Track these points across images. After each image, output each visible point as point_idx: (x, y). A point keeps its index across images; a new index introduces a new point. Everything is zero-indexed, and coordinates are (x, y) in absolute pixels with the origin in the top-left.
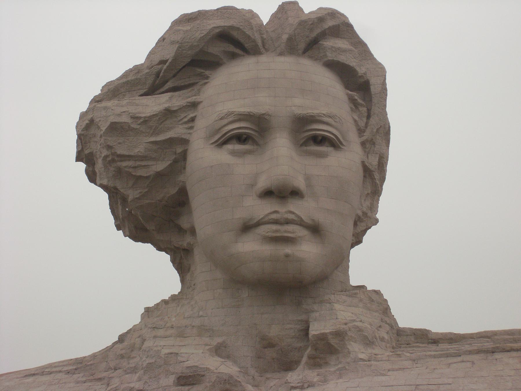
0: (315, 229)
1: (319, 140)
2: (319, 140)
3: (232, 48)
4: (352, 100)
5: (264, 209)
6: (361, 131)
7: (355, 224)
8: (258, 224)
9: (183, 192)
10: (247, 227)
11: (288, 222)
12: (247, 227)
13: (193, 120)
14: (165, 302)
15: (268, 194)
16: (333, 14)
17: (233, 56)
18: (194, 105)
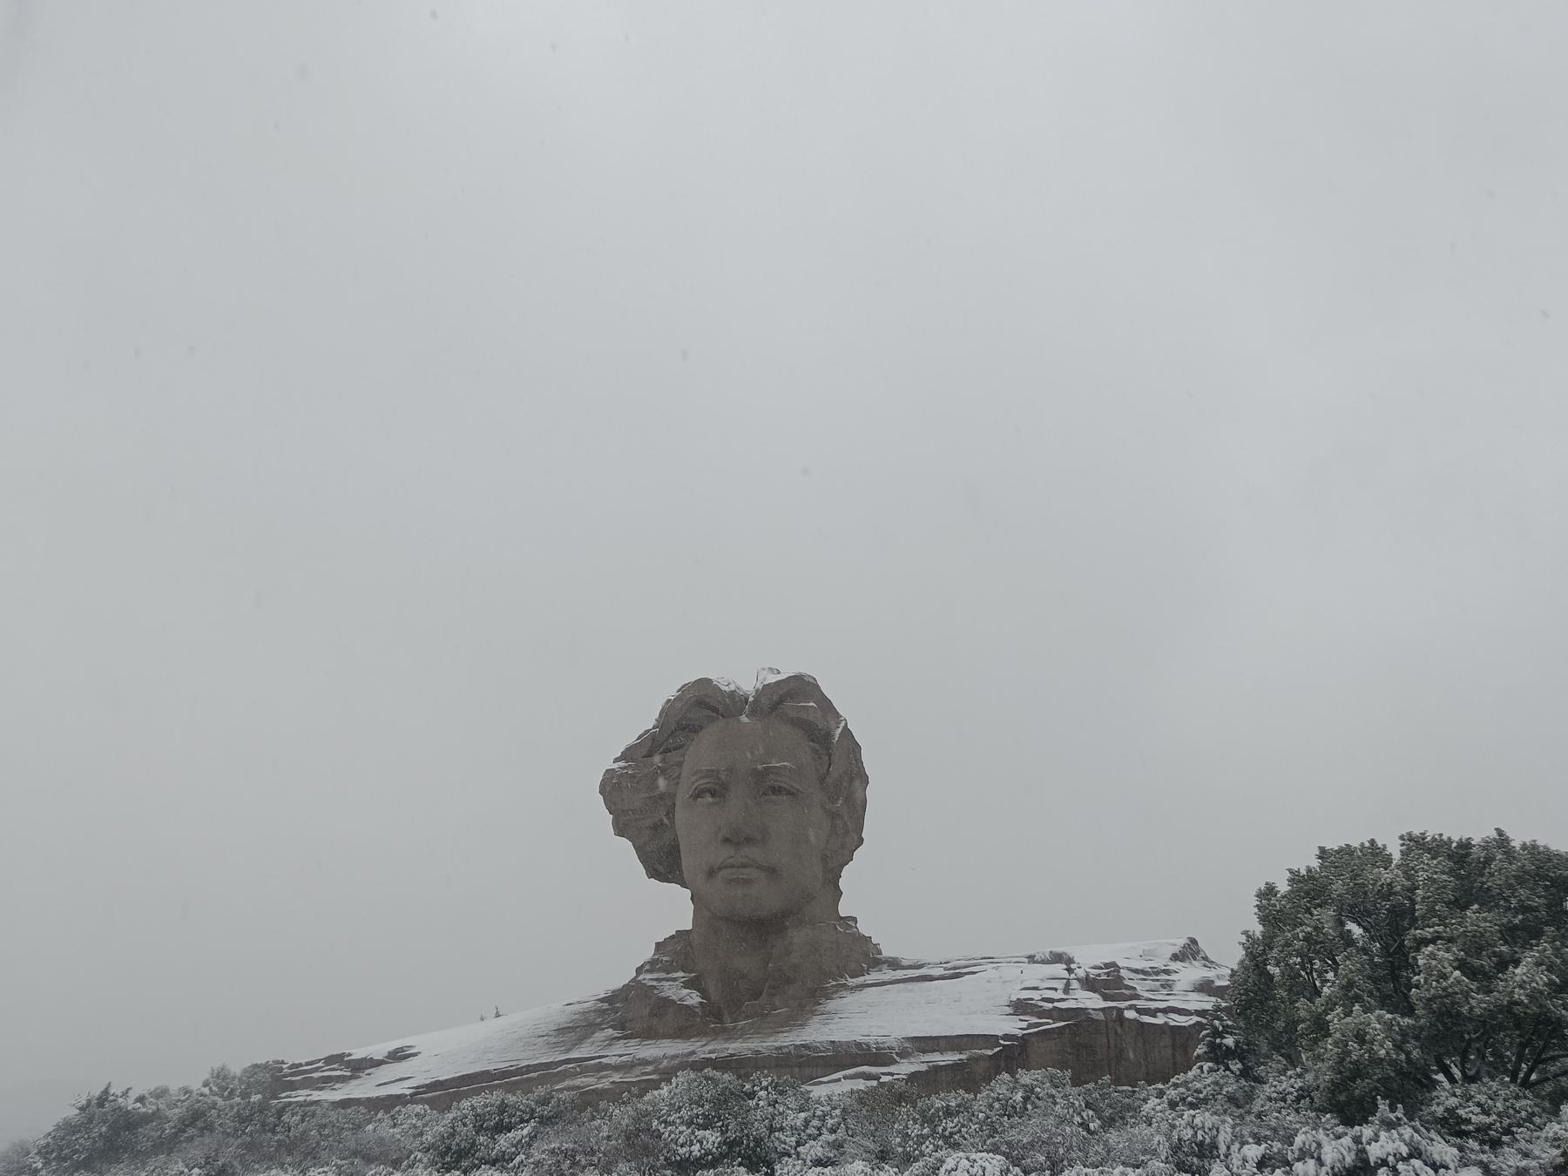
0: (772, 871)
1: (777, 790)
2: (777, 790)
3: (709, 712)
4: (815, 751)
5: (724, 854)
6: (822, 780)
7: (824, 859)
8: (720, 869)
9: (676, 839)
10: (711, 873)
11: (744, 866)
12: (711, 873)
13: (679, 777)
14: (672, 937)
15: (726, 840)
16: (798, 678)
17: (712, 720)
18: (680, 764)
